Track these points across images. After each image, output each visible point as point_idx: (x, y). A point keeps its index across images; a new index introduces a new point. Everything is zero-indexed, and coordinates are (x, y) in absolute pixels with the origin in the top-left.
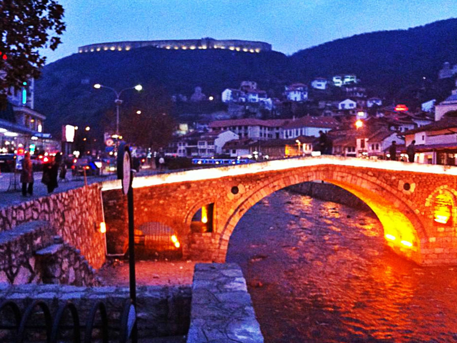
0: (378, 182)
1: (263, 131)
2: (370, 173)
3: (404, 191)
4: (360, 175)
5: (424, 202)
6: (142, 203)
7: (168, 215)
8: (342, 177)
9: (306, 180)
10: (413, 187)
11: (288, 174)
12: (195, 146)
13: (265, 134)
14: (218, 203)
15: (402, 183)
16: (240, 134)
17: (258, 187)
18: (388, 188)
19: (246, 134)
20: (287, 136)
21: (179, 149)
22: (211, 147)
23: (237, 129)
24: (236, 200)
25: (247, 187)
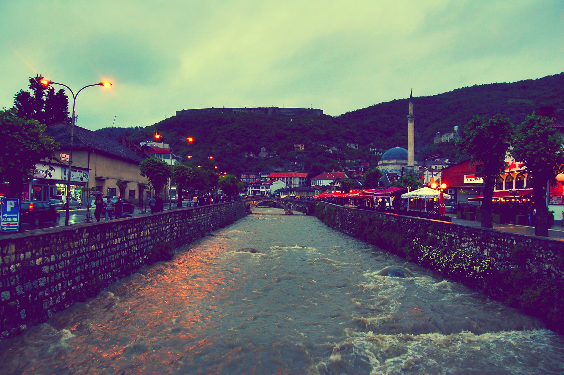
1: (302, 181)
13: (303, 183)
16: (287, 183)
19: (291, 182)
20: (318, 184)
22: (268, 190)
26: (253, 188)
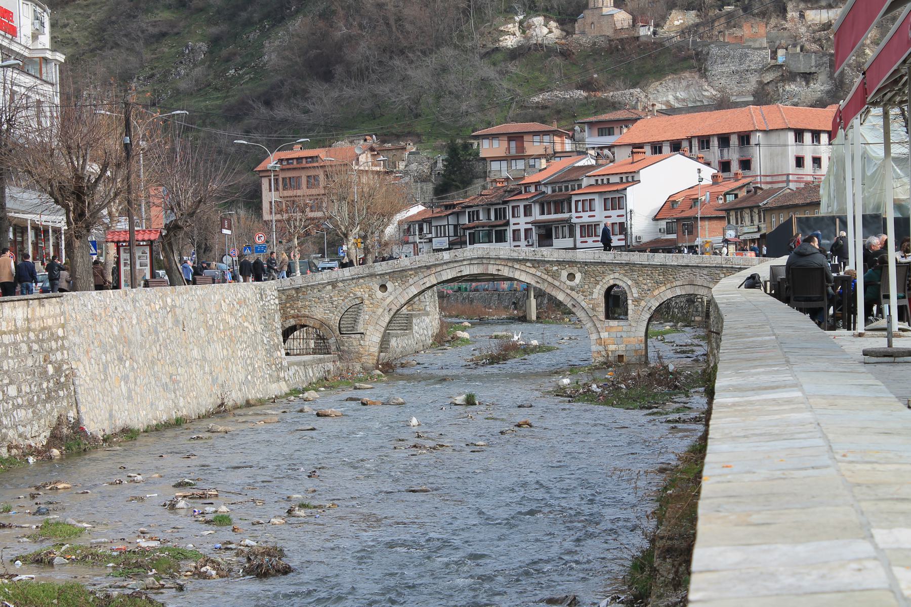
0: (539, 274)
2: (528, 264)
3: (568, 283)
4: (517, 266)
5: (591, 293)
6: (288, 305)
7: (315, 317)
8: (499, 270)
9: (459, 275)
10: (578, 276)
11: (439, 269)
12: (566, 216)
14: (367, 302)
15: (564, 274)
17: (407, 284)
18: (550, 279)
19: (746, 164)
21: (513, 227)
23: (715, 142)
24: (383, 299)
25: (397, 284)
26: (536, 209)
